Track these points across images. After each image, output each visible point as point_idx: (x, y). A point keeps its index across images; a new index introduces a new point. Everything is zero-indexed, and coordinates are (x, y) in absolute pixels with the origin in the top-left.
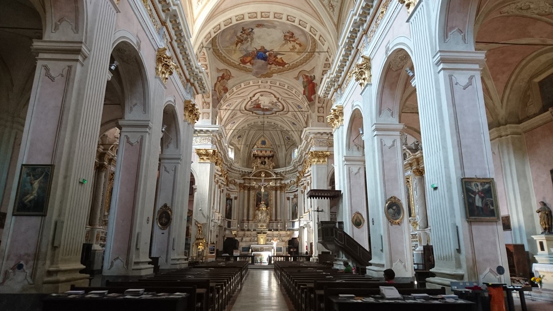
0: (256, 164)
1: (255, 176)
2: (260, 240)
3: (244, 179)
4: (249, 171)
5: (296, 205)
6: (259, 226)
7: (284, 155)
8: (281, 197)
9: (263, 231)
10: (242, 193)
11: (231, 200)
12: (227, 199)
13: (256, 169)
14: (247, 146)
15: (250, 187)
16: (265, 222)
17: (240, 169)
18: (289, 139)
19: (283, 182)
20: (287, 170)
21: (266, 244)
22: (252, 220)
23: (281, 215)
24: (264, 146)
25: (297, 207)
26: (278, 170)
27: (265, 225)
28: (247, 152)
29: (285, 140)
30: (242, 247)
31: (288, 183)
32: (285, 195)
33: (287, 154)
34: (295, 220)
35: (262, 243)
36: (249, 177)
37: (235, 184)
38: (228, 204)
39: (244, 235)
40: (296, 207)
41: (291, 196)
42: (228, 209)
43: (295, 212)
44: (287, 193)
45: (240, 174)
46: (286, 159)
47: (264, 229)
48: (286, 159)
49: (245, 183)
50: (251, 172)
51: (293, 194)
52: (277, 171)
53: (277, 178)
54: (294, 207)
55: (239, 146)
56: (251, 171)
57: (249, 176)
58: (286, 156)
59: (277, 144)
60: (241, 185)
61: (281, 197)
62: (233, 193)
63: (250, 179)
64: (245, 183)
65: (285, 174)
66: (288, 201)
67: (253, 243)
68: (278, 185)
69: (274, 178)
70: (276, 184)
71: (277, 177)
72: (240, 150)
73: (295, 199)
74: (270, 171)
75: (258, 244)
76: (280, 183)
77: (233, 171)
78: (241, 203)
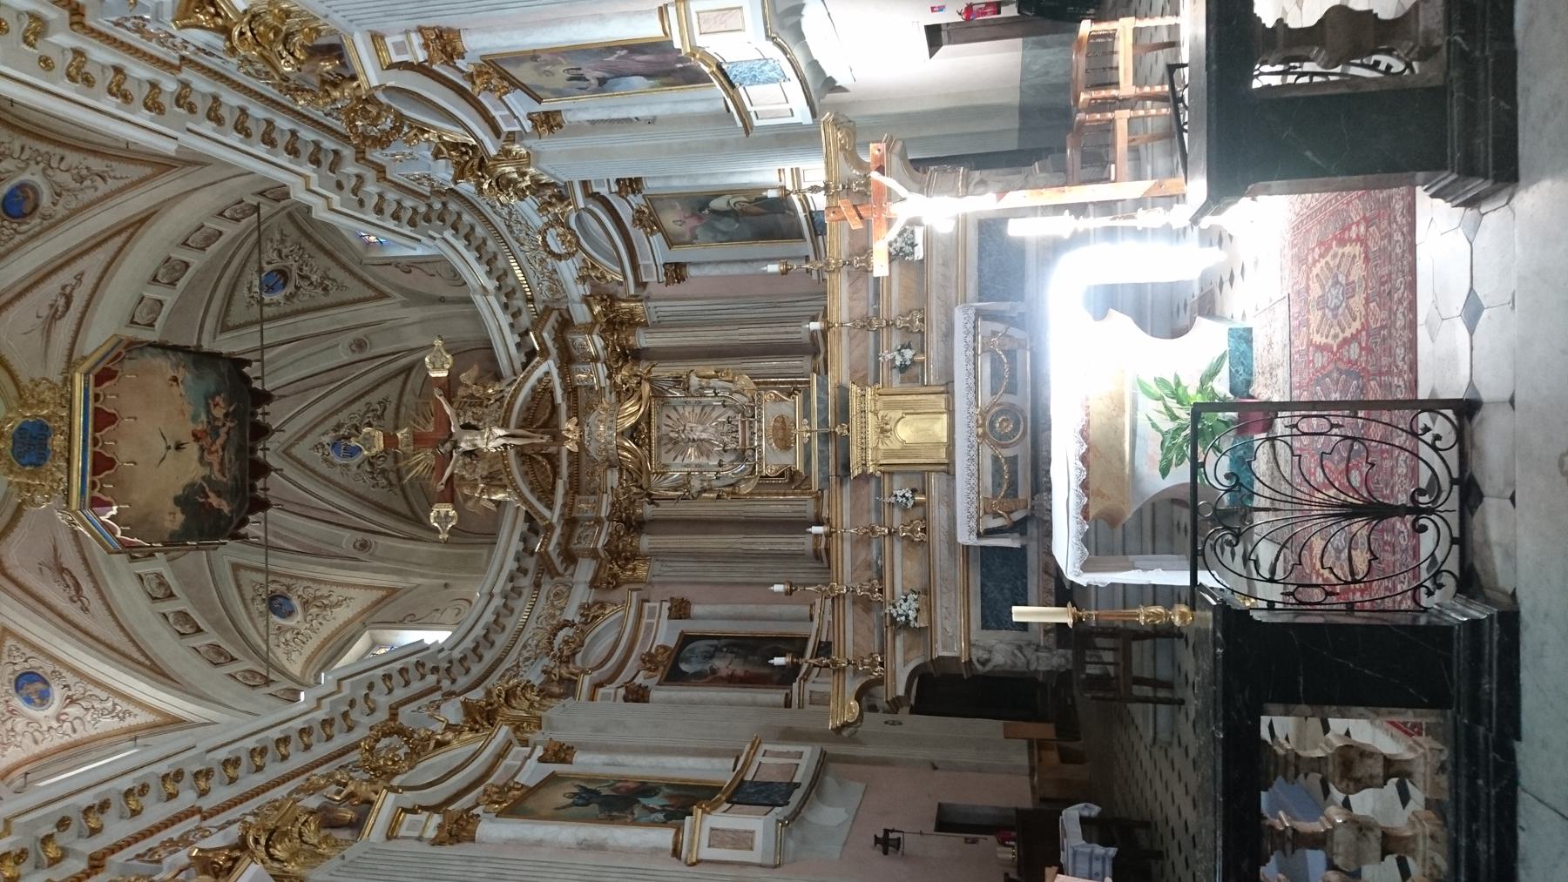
0: (476, 486)
1: (547, 496)
2: (906, 448)
3: (570, 558)
4: (521, 526)
5: (699, 204)
6: (786, 459)
7: (415, 313)
8: (679, 323)
9: (823, 422)
10: (657, 566)
11: (686, 639)
12: (674, 676)
13: (504, 487)
14: (364, 546)
15: (620, 520)
16: (749, 413)
17: (497, 590)
18: (283, 274)
19: (581, 314)
20: (491, 285)
21: (948, 389)
22: (819, 499)
23: (781, 321)
24: (57, 441)
25: (718, 204)
26: (506, 345)
27: (772, 408)
28: (410, 545)
29: (297, 304)
30: (977, 634)
31: (583, 279)
32: (664, 301)
33: (401, 290)
34: (801, 215)
35: (940, 428)
36: (558, 531)
37: (590, 615)
38: (707, 667)
39: (866, 604)
40: (717, 213)
41: (653, 251)
42: (739, 669)
43: (744, 213)
44: (641, 285)
45: (537, 585)
46: (442, 300)
47: (807, 414)
48: (442, 300)
49: (594, 554)
50: (529, 518)
51: (637, 234)
52: (513, 350)
53: (553, 351)
54: (722, 225)
55: (362, 599)
56: (522, 516)
57: (550, 528)
58: (416, 298)
59: (345, 357)
60: (604, 575)
61: (679, 323)
62: (649, 626)
63: (571, 522)
64: (594, 554)
65: (531, 300)
66: (692, 272)
67: (938, 514)
68: (599, 342)
69: (555, 372)
70: (596, 359)
71: (545, 353)
72: (393, 591)
73: (670, 219)
74: (514, 396)
75: (948, 469)
76: (589, 329)
77: (501, 640)
78: (715, 573)
